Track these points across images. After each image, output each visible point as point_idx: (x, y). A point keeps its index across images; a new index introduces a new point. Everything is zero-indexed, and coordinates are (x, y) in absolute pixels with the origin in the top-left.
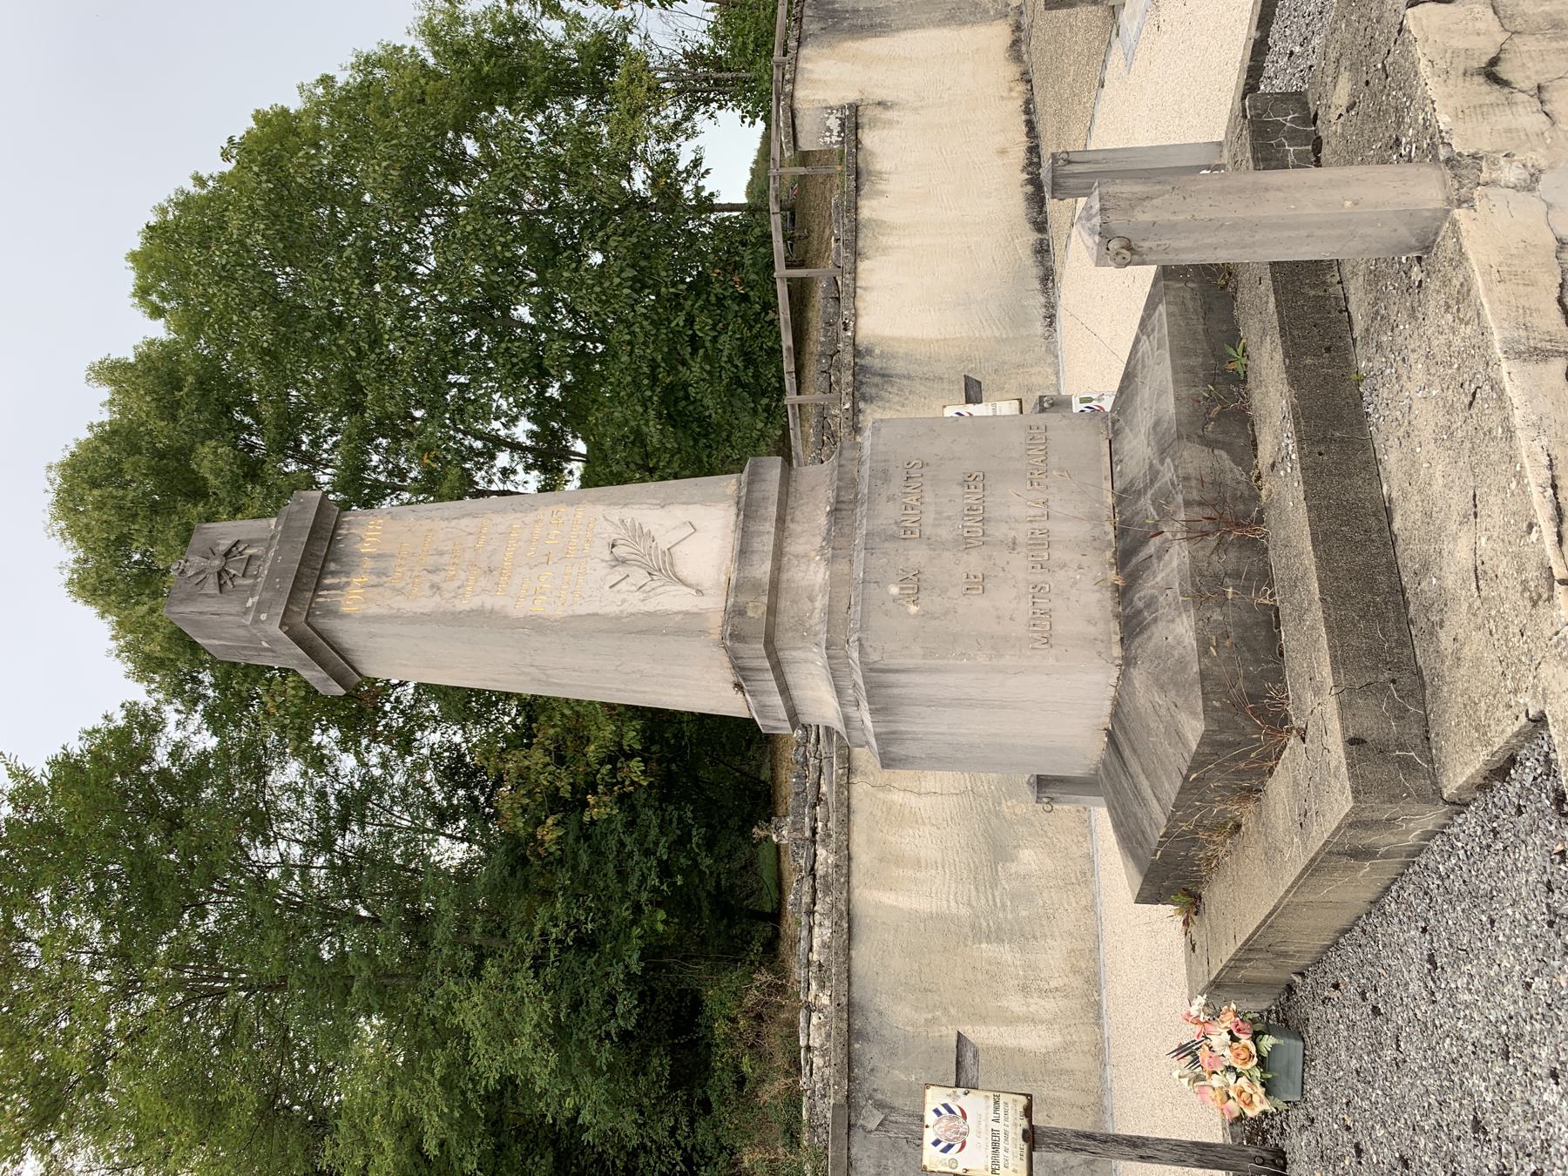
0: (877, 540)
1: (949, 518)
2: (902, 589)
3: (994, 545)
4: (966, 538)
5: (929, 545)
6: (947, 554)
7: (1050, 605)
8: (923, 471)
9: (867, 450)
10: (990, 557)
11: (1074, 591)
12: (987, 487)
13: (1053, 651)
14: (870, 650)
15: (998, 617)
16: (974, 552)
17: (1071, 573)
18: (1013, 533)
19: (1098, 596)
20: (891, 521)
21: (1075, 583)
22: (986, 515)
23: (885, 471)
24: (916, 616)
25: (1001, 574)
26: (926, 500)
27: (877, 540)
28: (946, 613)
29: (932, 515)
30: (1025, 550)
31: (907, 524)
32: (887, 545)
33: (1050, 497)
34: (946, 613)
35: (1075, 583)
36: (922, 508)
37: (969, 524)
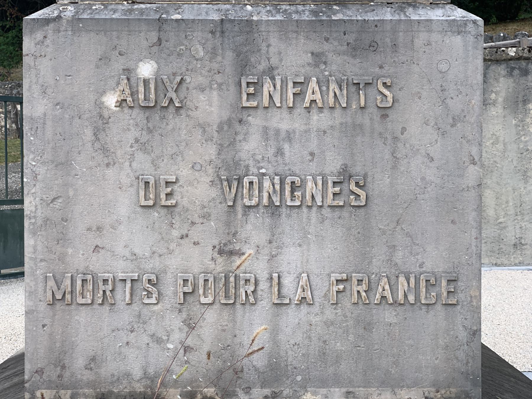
0: (239, 39)
1: (280, 152)
2: (146, 82)
3: (228, 224)
4: (240, 180)
5: (229, 123)
6: (211, 151)
7: (121, 305)
8: (372, 109)
9: (414, 15)
10: (206, 216)
11: (146, 339)
12: (337, 213)
13: (42, 307)
14: (39, 36)
15: (99, 229)
16: (214, 192)
17: (177, 336)
18: (249, 251)
19: (137, 373)
20: (274, 61)
21: (159, 341)
22: (284, 210)
23: (373, 47)
24: (100, 105)
25: (176, 233)
26: (315, 117)
27: (239, 39)
28: (104, 150)
29: (284, 126)
30: (219, 269)
31: (267, 87)
32: (230, 55)
33: (316, 309)
34: (104, 150)
35: (159, 341)
36: (299, 110)
37: (267, 184)
